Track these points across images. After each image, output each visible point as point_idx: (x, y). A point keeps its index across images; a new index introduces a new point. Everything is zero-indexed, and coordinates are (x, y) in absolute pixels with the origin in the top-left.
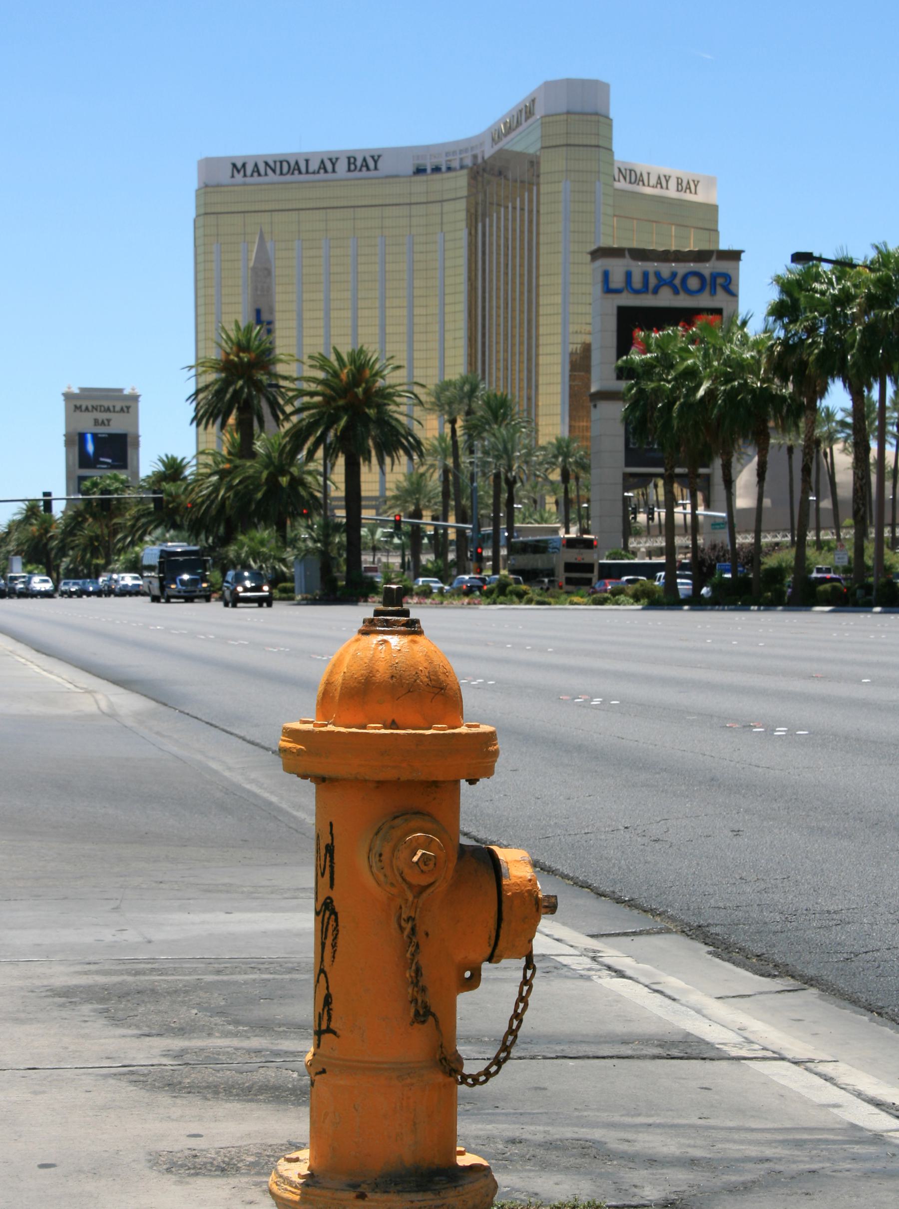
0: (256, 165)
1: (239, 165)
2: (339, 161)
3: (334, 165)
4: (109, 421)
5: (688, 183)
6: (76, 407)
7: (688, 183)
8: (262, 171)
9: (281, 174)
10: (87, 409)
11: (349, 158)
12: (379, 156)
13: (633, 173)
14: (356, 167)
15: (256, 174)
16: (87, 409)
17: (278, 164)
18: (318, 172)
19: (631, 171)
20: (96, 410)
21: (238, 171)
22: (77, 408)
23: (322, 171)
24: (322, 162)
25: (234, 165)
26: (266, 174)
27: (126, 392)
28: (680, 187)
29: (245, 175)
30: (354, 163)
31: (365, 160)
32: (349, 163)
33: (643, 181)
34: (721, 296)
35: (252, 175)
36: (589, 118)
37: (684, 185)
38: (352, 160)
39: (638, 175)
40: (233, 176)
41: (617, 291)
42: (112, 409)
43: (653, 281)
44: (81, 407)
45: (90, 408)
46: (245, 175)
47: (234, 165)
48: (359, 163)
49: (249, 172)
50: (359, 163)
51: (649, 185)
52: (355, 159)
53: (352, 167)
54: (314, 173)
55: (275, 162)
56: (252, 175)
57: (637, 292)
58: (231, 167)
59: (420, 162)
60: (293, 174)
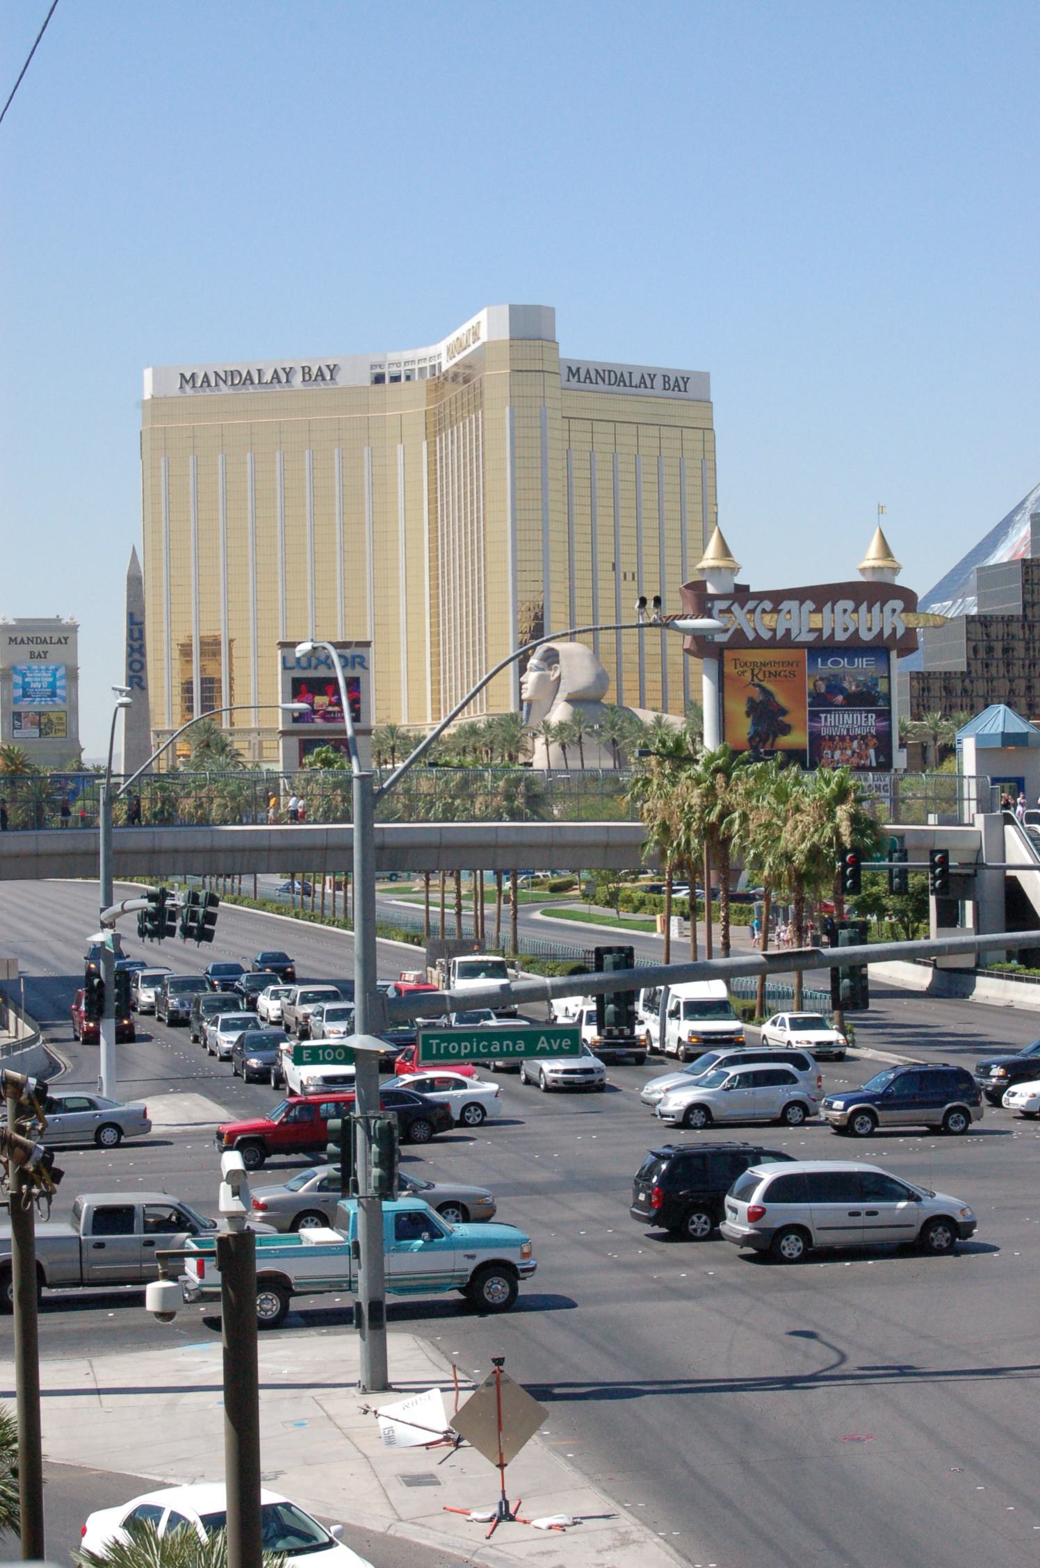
0: (206, 375)
1: (188, 376)
4: (45, 653)
5: (677, 380)
6: (10, 638)
7: (677, 380)
8: (213, 384)
11: (303, 368)
13: (612, 374)
19: (609, 371)
21: (187, 382)
24: (276, 371)
27: (64, 622)
28: (667, 386)
29: (194, 386)
30: (309, 373)
31: (320, 368)
32: (304, 373)
33: (624, 381)
34: (358, 669)
36: (532, 342)
37: (672, 383)
38: (307, 370)
39: (619, 376)
41: (290, 668)
42: (49, 641)
43: (314, 661)
45: (26, 641)
46: (194, 386)
47: (182, 375)
49: (199, 383)
51: (631, 386)
53: (307, 378)
55: (226, 372)
57: (305, 669)
58: (179, 377)
59: (378, 370)
60: (244, 384)
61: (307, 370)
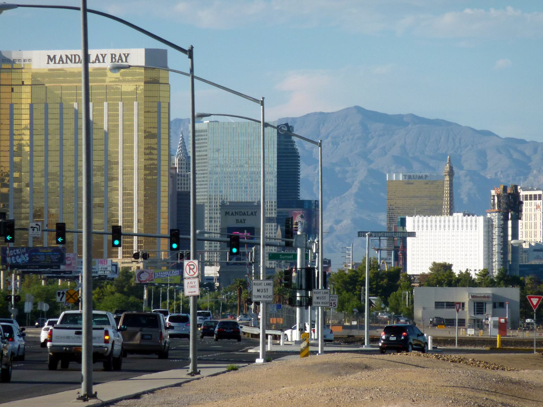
1: (52, 57)
2: (106, 55)
3: (104, 58)
8: (65, 61)
9: (75, 62)
10: (232, 214)
11: (112, 55)
12: (128, 54)
14: (115, 59)
15: (61, 62)
17: (73, 56)
18: (95, 62)
21: (52, 61)
22: (227, 213)
23: (97, 61)
25: (49, 57)
26: (67, 62)
29: (55, 63)
30: (115, 58)
31: (120, 56)
35: (59, 63)
38: (114, 56)
40: (48, 63)
44: (229, 212)
45: (234, 214)
47: (49, 57)
48: (117, 58)
49: (57, 62)
50: (117, 58)
52: (115, 55)
53: (114, 60)
54: (93, 63)
61: (114, 56)
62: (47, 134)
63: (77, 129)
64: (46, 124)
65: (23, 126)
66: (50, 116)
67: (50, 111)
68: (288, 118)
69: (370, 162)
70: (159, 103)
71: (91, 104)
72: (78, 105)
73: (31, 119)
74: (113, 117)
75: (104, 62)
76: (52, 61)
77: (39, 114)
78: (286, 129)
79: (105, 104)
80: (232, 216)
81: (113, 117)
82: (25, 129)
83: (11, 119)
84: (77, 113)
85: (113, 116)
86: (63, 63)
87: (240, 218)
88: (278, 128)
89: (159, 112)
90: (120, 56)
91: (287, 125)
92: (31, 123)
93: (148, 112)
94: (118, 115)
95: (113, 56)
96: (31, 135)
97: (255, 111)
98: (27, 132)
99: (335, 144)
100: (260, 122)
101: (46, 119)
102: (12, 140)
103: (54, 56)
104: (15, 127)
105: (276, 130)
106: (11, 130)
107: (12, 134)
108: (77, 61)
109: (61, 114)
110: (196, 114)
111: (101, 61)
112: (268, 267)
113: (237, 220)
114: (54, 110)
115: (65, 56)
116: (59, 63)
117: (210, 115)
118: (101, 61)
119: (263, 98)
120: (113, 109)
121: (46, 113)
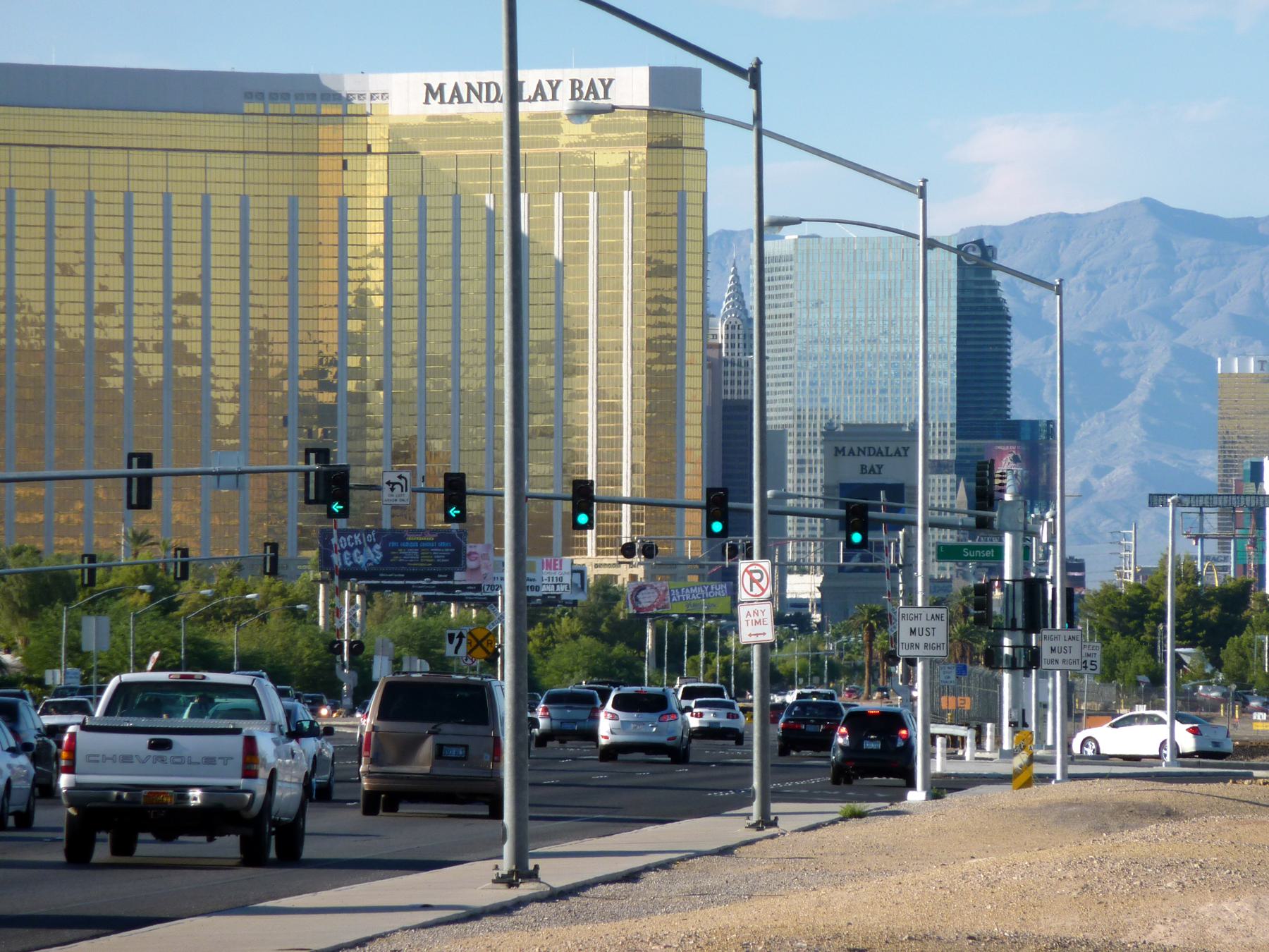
1: (435, 88)
2: (561, 84)
3: (554, 90)
8: (465, 99)
9: (488, 100)
10: (852, 452)
11: (573, 81)
12: (611, 81)
14: (581, 93)
15: (456, 100)
16: (852, 452)
17: (484, 86)
18: (535, 99)
20: (864, 453)
21: (434, 98)
22: (839, 451)
23: (539, 98)
25: (429, 87)
26: (469, 101)
30: (579, 89)
31: (592, 83)
38: (577, 85)
44: (843, 449)
45: (856, 453)
46: (442, 102)
47: (429, 87)
48: (585, 89)
49: (447, 99)
50: (585, 89)
52: (581, 83)
54: (529, 100)
56: (451, 102)
61: (577, 85)
62: (423, 267)
63: (492, 254)
64: (422, 244)
65: (369, 249)
66: (430, 226)
67: (430, 214)
68: (981, 228)
69: (1178, 329)
70: (682, 194)
71: (524, 198)
72: (495, 199)
73: (388, 233)
74: (574, 227)
75: (554, 98)
76: (434, 98)
77: (406, 221)
78: (978, 253)
79: (558, 197)
80: (851, 457)
81: (574, 227)
82: (375, 254)
83: (343, 233)
84: (491, 217)
85: (576, 223)
86: (461, 101)
87: (870, 461)
88: (960, 250)
89: (681, 215)
90: (592, 83)
91: (980, 243)
92: (388, 243)
93: (656, 215)
94: (586, 223)
95: (575, 85)
96: (388, 269)
97: (906, 213)
98: (379, 263)
99: (1094, 287)
100: (916, 237)
101: (422, 232)
102: (343, 281)
103: (441, 87)
104: (351, 251)
105: (954, 256)
106: (343, 257)
107: (343, 268)
108: (492, 98)
109: (457, 219)
110: (766, 219)
111: (549, 96)
112: (936, 577)
113: (862, 466)
114: (440, 213)
115: (466, 86)
116: (451, 102)
117: (802, 220)
118: (549, 96)
119: (925, 181)
120: (574, 207)
121: (422, 219)
